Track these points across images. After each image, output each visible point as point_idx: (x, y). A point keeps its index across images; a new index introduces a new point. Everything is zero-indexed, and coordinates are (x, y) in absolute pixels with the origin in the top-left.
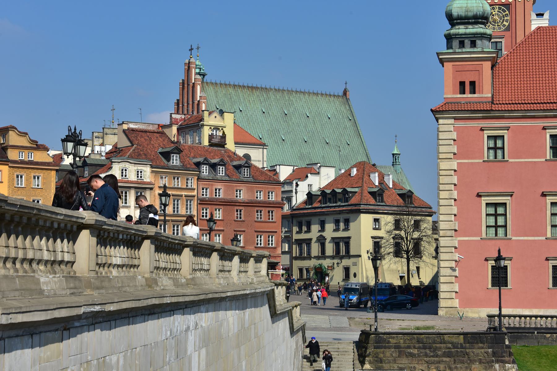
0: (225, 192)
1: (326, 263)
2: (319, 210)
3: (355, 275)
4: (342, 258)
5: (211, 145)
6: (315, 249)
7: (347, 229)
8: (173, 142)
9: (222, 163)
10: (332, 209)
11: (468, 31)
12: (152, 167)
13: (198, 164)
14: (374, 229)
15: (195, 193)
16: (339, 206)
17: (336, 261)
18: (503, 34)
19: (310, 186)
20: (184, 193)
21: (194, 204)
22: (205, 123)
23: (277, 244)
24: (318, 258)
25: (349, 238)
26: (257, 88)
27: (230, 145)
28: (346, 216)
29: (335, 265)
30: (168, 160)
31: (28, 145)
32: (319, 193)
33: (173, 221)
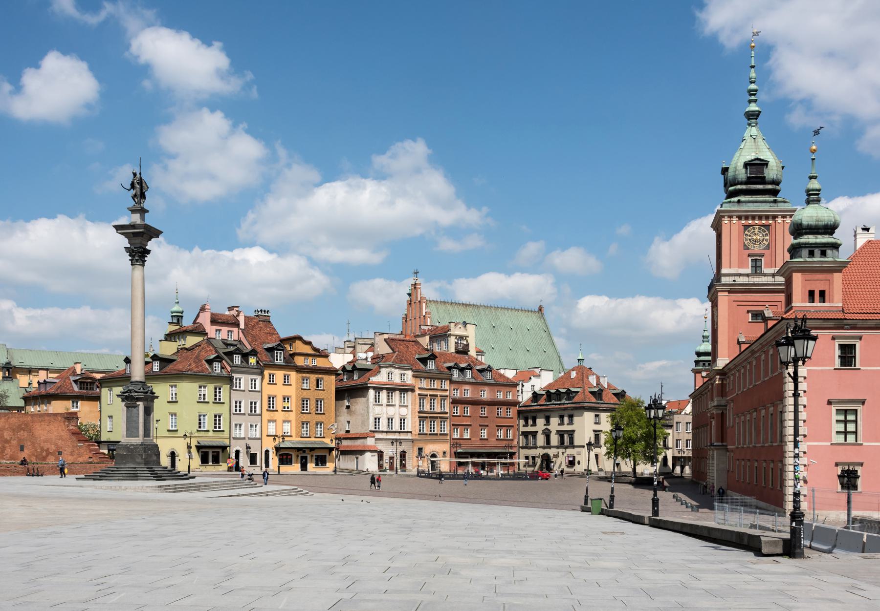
0: (472, 392)
1: (551, 452)
2: (544, 407)
3: (579, 463)
4: (566, 448)
5: (458, 352)
6: (541, 440)
7: (571, 423)
8: (427, 350)
9: (469, 368)
10: (557, 406)
11: (818, 241)
12: (412, 370)
13: (450, 368)
14: (596, 423)
15: (447, 393)
16: (564, 404)
17: (561, 450)
18: (763, 252)
19: (533, 386)
20: (439, 393)
21: (447, 403)
22: (452, 333)
23: (514, 435)
24: (543, 447)
25: (574, 431)
26: (470, 305)
27: (472, 352)
28: (571, 412)
29: (560, 454)
30: (426, 365)
31: (313, 352)
32: (544, 393)
33: (430, 417)
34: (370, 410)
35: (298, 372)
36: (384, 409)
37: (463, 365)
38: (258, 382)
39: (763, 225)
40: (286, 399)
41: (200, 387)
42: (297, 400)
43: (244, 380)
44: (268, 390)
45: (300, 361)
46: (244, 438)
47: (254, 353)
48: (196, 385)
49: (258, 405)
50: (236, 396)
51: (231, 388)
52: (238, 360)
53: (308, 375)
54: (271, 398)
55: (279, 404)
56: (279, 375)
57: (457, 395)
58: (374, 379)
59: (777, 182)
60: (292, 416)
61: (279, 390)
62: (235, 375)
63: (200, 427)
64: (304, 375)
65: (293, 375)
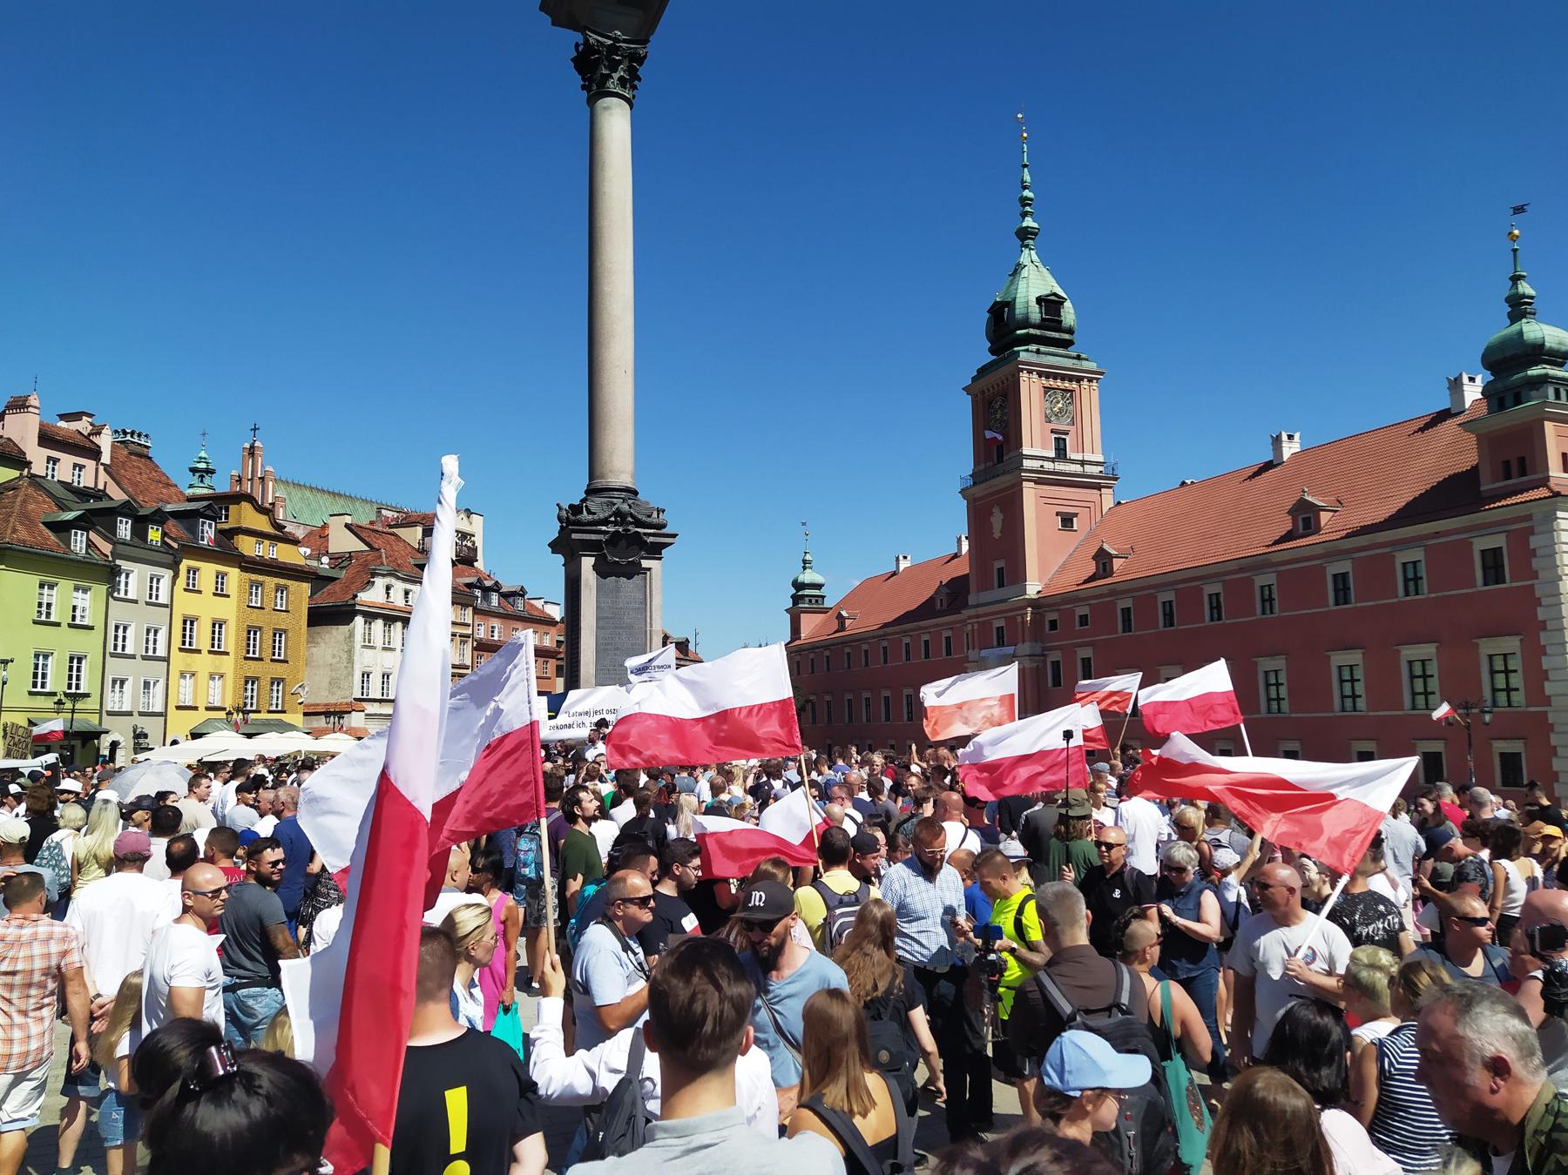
13: (469, 586)
21: (468, 648)
26: (339, 495)
31: (271, 530)
34: (356, 658)
35: (244, 569)
36: (379, 653)
37: (488, 583)
38: (165, 584)
39: (1066, 391)
40: (218, 624)
41: (42, 586)
42: (237, 631)
43: (136, 577)
44: (186, 604)
45: (248, 546)
46: (130, 714)
47: (159, 518)
48: (33, 580)
49: (162, 636)
50: (118, 612)
51: (110, 594)
52: (124, 529)
53: (261, 578)
54: (189, 621)
55: (202, 638)
56: (208, 570)
57: (481, 634)
58: (363, 597)
59: (1070, 331)
60: (228, 665)
61: (205, 607)
62: (124, 565)
63: (35, 685)
64: (254, 577)
65: (234, 574)
